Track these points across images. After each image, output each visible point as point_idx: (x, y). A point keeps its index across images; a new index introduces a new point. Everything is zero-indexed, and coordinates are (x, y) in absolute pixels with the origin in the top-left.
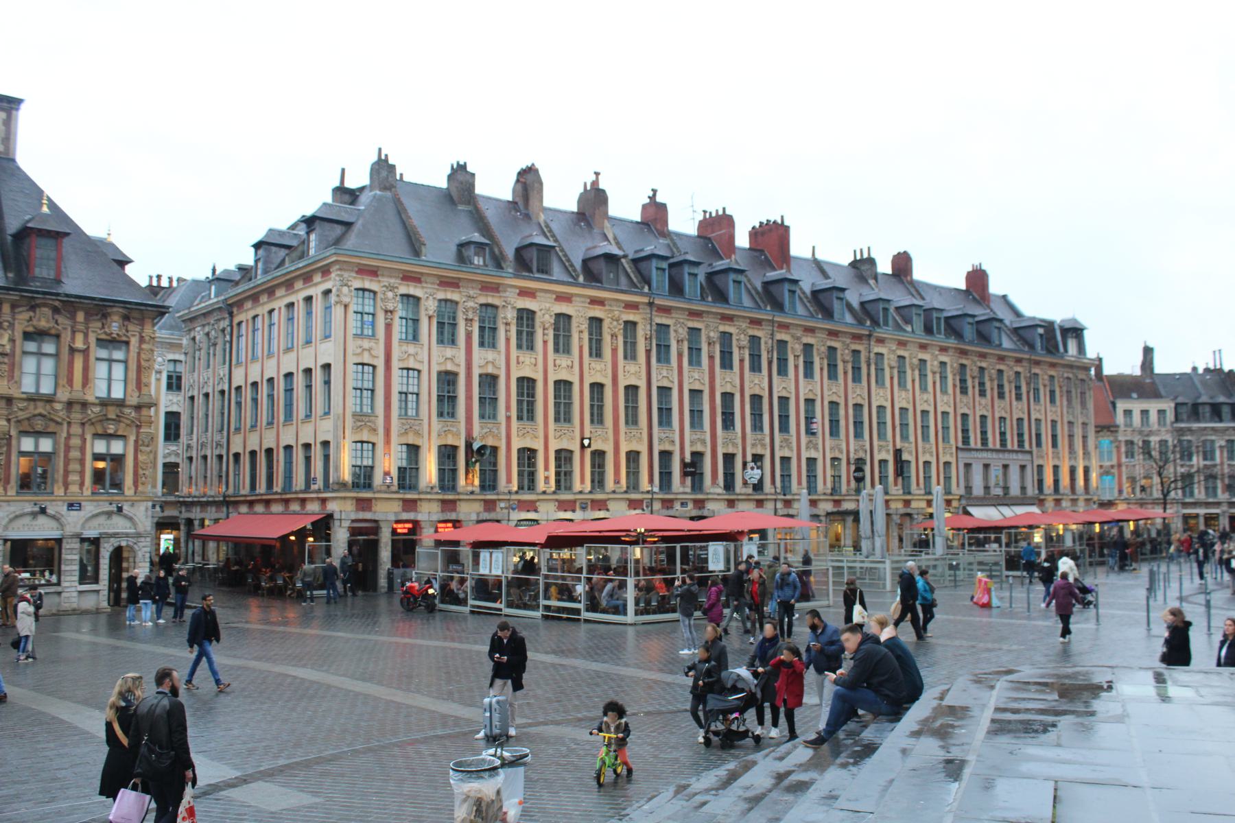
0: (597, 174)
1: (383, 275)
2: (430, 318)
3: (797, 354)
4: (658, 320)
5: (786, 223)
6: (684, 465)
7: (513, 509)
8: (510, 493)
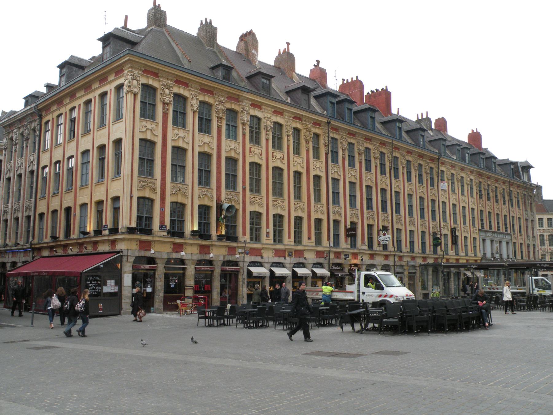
0: (288, 44)
1: (162, 77)
2: (194, 112)
3: (403, 165)
4: (331, 135)
5: (389, 90)
6: (347, 230)
7: (247, 254)
8: (245, 242)
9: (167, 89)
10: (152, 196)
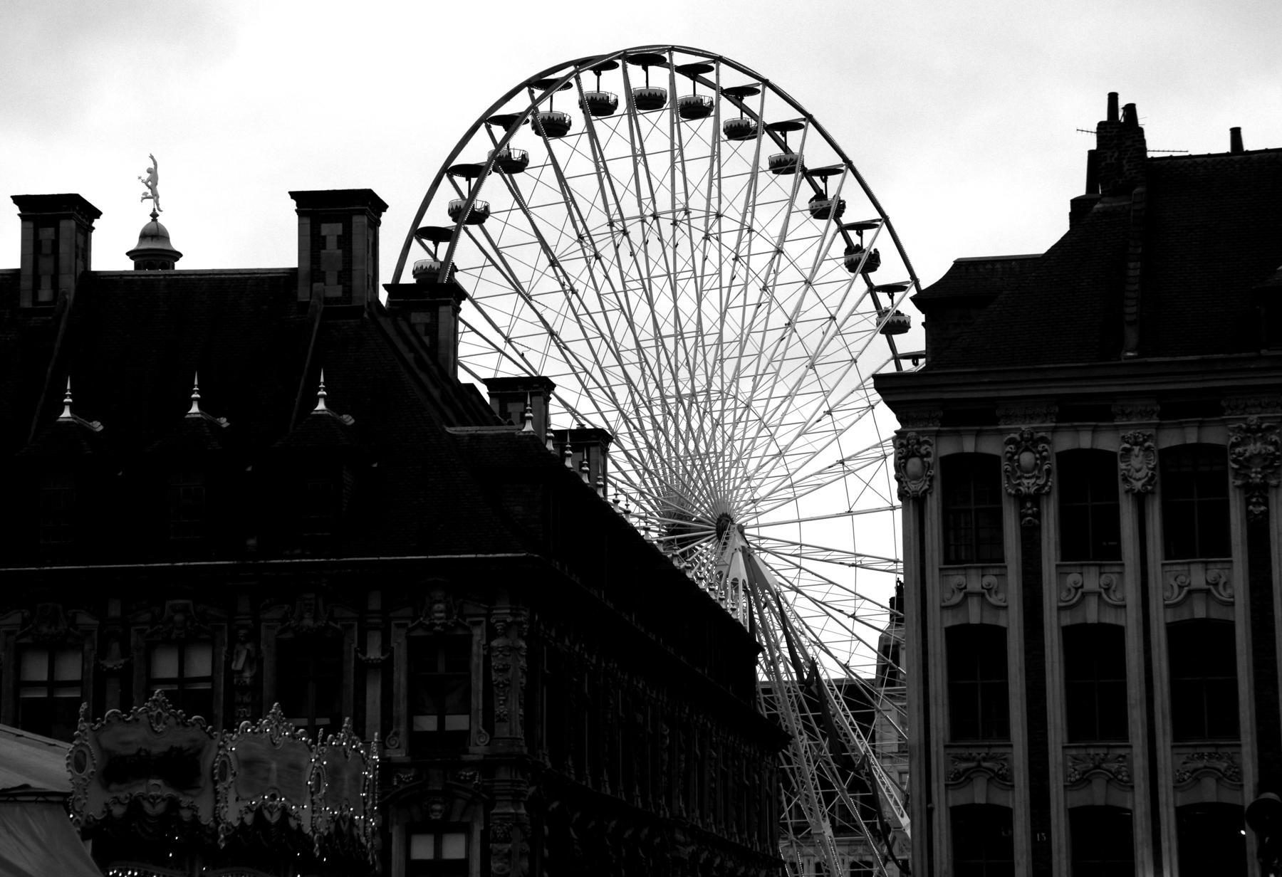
9: (1027, 449)
10: (1000, 799)
